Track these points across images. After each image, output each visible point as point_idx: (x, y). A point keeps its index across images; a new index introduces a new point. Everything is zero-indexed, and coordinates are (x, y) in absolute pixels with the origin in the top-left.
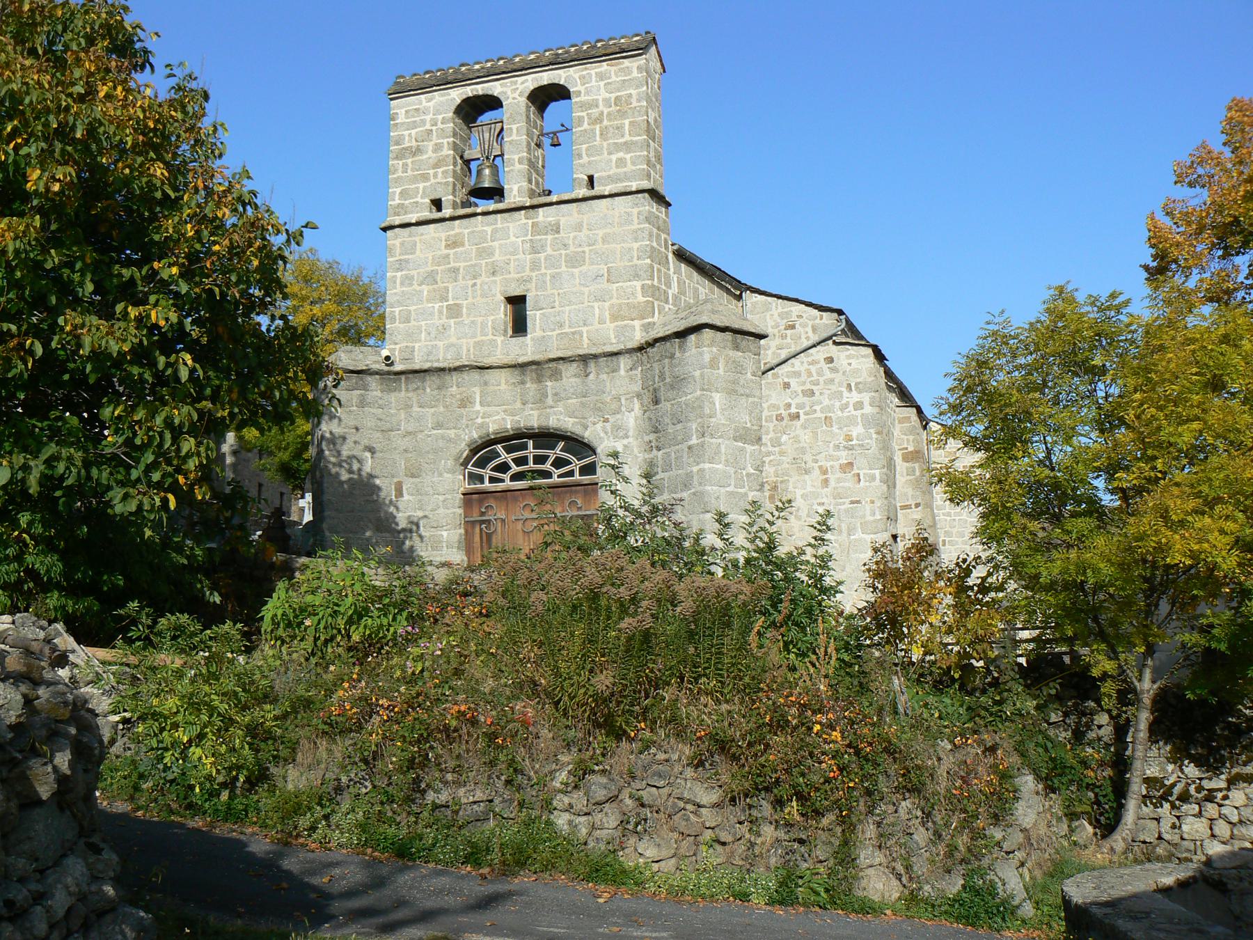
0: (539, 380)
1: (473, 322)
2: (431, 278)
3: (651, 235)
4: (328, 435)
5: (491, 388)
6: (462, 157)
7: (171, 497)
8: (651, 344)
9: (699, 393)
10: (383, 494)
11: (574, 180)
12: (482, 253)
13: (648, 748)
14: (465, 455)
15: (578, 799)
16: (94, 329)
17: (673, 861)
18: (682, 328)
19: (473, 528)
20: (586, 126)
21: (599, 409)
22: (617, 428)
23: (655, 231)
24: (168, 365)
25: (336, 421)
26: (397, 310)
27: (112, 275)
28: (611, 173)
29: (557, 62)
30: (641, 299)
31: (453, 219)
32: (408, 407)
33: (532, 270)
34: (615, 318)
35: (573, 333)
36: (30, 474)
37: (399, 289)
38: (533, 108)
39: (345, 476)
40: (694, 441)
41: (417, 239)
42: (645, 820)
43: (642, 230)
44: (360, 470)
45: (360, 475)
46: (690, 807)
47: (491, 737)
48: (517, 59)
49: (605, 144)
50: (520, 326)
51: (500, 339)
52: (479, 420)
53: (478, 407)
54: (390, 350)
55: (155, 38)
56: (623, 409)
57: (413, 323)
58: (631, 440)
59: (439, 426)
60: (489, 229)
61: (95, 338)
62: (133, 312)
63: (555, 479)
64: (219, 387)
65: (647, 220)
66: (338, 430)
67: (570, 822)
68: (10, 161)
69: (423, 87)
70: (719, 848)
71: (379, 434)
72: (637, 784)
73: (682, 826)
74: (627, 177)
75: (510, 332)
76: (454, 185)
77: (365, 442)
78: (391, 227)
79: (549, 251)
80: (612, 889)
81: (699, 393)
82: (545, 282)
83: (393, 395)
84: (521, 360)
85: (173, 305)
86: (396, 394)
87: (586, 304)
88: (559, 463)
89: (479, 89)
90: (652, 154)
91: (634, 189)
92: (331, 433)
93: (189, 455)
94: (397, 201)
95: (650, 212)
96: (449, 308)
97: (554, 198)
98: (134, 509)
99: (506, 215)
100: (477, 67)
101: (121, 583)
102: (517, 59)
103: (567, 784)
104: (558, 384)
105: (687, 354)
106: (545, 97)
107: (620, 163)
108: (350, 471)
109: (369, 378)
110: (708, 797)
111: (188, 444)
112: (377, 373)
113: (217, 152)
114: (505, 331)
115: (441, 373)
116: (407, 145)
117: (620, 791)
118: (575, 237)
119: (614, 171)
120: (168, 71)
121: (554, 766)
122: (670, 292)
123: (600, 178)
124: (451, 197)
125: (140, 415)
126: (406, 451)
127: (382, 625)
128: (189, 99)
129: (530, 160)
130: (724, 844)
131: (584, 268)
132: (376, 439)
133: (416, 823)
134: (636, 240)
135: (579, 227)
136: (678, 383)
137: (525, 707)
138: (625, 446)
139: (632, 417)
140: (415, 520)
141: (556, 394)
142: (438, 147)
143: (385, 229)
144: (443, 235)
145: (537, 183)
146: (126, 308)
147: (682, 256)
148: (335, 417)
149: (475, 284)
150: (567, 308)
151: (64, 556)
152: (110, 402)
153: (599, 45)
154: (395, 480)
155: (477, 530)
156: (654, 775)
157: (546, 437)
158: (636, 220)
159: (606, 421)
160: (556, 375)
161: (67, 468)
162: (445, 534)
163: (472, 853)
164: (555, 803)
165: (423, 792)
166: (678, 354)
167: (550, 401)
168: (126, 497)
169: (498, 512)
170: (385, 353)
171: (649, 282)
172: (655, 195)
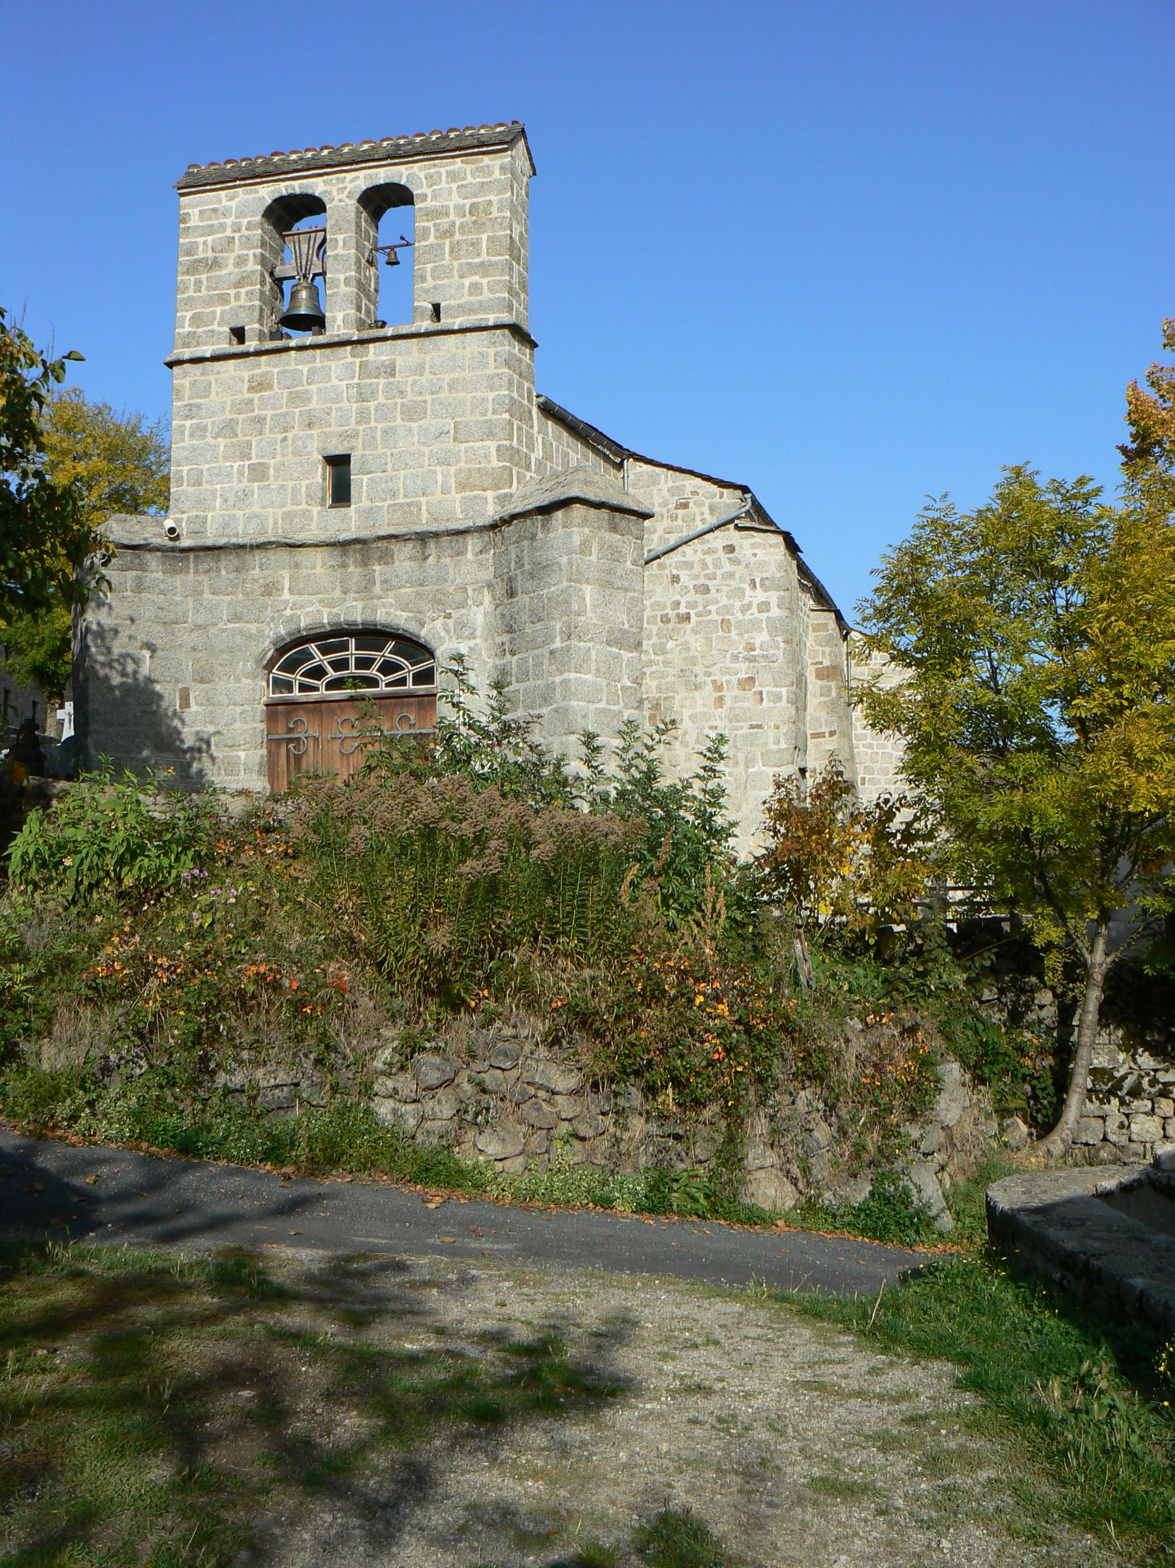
0: (365, 562)
1: (282, 487)
2: (229, 428)
4: (94, 627)
5: (304, 571)
6: (271, 274)
9: (565, 584)
10: (164, 704)
11: (417, 308)
13: (490, 1022)
15: (405, 1083)
17: (521, 1159)
18: (546, 502)
20: (432, 239)
21: (440, 602)
22: (461, 625)
23: (516, 377)
25: (106, 609)
26: (185, 469)
28: (463, 301)
29: (397, 155)
30: (495, 463)
31: (258, 353)
32: (198, 593)
33: (358, 423)
34: (462, 486)
35: (410, 505)
37: (187, 442)
38: (364, 214)
39: (116, 680)
40: (557, 644)
41: (212, 378)
42: (488, 1109)
44: (135, 672)
45: (136, 679)
46: (542, 1094)
47: (297, 1006)
48: (346, 150)
49: (456, 264)
50: (341, 494)
51: (316, 510)
52: (288, 612)
53: (286, 595)
54: (176, 520)
56: (470, 602)
57: (205, 486)
58: (478, 641)
59: (236, 618)
60: (304, 369)
63: (383, 688)
65: (507, 363)
66: (107, 621)
67: (394, 1111)
70: (577, 1144)
71: (160, 628)
72: (478, 1066)
73: (533, 1117)
74: (482, 308)
75: (329, 501)
76: (261, 310)
77: (142, 637)
78: (180, 362)
79: (381, 399)
80: (445, 1192)
81: (565, 584)
84: (342, 537)
86: (183, 576)
87: (426, 467)
88: (388, 668)
89: (296, 187)
90: (515, 280)
91: (491, 323)
92: (99, 624)
94: (187, 329)
97: (389, 331)
99: (327, 351)
100: (294, 157)
102: (346, 150)
103: (391, 1065)
107: (475, 288)
108: (124, 674)
109: (148, 556)
110: (564, 1082)
112: (158, 549)
114: (323, 499)
115: (240, 552)
116: (201, 255)
117: (456, 1074)
118: (414, 383)
119: (466, 298)
121: (375, 1042)
122: (533, 457)
124: (257, 326)
126: (194, 649)
129: (359, 281)
130: (583, 1139)
131: (424, 423)
133: (203, 1111)
134: (491, 388)
135: (419, 370)
136: (540, 571)
137: (339, 970)
138: (471, 649)
139: (481, 613)
140: (206, 736)
141: (385, 581)
142: (241, 261)
143: (170, 365)
144: (246, 375)
145: (368, 312)
147: (549, 410)
148: (104, 604)
149: (285, 439)
153: (452, 135)
154: (180, 686)
156: (498, 1054)
157: (372, 636)
159: (448, 616)
160: (386, 558)
162: (242, 755)
163: (273, 1148)
164: (376, 1087)
165: (213, 1074)
166: (540, 535)
167: (377, 589)
169: (309, 729)
170: (169, 523)
171: (507, 443)
172: (518, 332)
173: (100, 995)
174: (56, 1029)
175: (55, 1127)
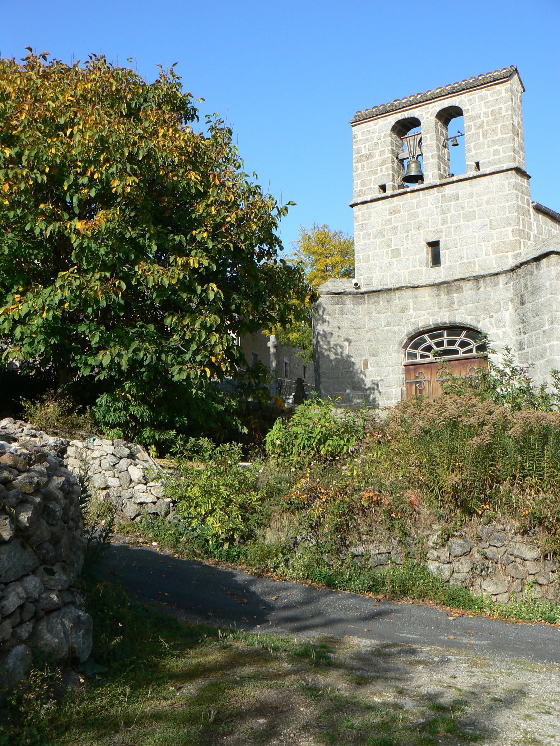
0: (449, 293)
1: (407, 259)
2: (381, 234)
3: (517, 197)
4: (321, 332)
5: (419, 300)
6: (397, 158)
7: (207, 370)
8: (519, 267)
9: (549, 296)
10: (356, 367)
11: (467, 166)
12: (411, 216)
13: (490, 522)
14: (405, 342)
15: (444, 553)
16: (156, 272)
17: (507, 594)
18: (537, 255)
19: (411, 386)
20: (473, 131)
21: (487, 310)
22: (498, 321)
23: (520, 194)
24: (203, 291)
25: (327, 323)
26: (361, 255)
27: (169, 241)
28: (491, 158)
29: (454, 92)
30: (511, 238)
31: (393, 196)
32: (370, 313)
33: (442, 225)
34: (495, 251)
35: (470, 263)
36: (122, 358)
37: (362, 242)
38: (440, 123)
39: (333, 357)
40: (547, 327)
41: (372, 210)
42: (488, 568)
43: (511, 194)
44: (342, 353)
45: (342, 356)
46: (518, 560)
47: (389, 513)
48: (429, 93)
49: (486, 141)
50: (436, 260)
51: (424, 269)
52: (413, 320)
53: (412, 312)
54: (358, 279)
55: (201, 101)
56: (502, 309)
57: (371, 262)
58: (507, 328)
59: (388, 324)
60: (415, 201)
61: (156, 277)
62: (180, 261)
63: (461, 355)
64: (240, 304)
65: (514, 187)
66: (327, 329)
67: (438, 568)
68: (104, 177)
69: (371, 117)
70: (538, 587)
71: (352, 331)
72: (483, 545)
73: (513, 572)
74: (500, 161)
75: (431, 264)
76: (393, 175)
77: (345, 336)
78: (356, 205)
79: (453, 212)
80: (461, 611)
81: (549, 296)
82: (451, 232)
83: (360, 306)
84: (437, 281)
85: (206, 256)
86: (362, 306)
87: (477, 243)
88: (463, 344)
89: (406, 115)
90: (517, 145)
91: (505, 168)
92: (323, 331)
93: (215, 345)
94: (359, 188)
95: (516, 183)
96: (392, 251)
97: (455, 178)
98: (185, 378)
99: (425, 191)
100: (404, 101)
101: (186, 422)
102: (429, 93)
103: (436, 544)
104: (460, 295)
105: (541, 272)
106: (448, 115)
107: (496, 152)
108: (336, 354)
109: (345, 297)
110: (530, 554)
111: (215, 338)
112: (350, 294)
113: (237, 165)
114: (427, 264)
115: (389, 292)
116: (363, 153)
117: (471, 549)
118: (469, 202)
119: (492, 158)
120: (207, 120)
121: (429, 532)
122: (532, 233)
123: (483, 163)
124: (391, 183)
125: (187, 321)
126: (369, 340)
127: (339, 445)
128: (222, 136)
129: (439, 156)
130: (541, 585)
131: (475, 221)
132: (351, 334)
133: (342, 565)
134: (507, 201)
135: (471, 195)
136: (536, 290)
137: (412, 495)
138: (504, 332)
139: (508, 314)
140: (376, 382)
141: (459, 302)
142: (382, 153)
143: (352, 206)
144: (387, 207)
145: (445, 170)
146: (176, 259)
147: (539, 209)
148: (325, 321)
149: (408, 236)
150: (465, 247)
151: (150, 407)
152: (169, 315)
153: (480, 78)
154: (363, 358)
155: (414, 387)
156: (494, 539)
157: (454, 329)
158: (507, 189)
159: (492, 317)
160: (459, 290)
161: (145, 354)
162: (394, 390)
163: (374, 585)
164: (428, 555)
165: (348, 547)
166: (535, 272)
167: (456, 306)
168: (181, 370)
169: (426, 376)
170: (354, 281)
171: (517, 227)
172: (518, 170)
173: (297, 508)
174: (272, 524)
175: (268, 571)
